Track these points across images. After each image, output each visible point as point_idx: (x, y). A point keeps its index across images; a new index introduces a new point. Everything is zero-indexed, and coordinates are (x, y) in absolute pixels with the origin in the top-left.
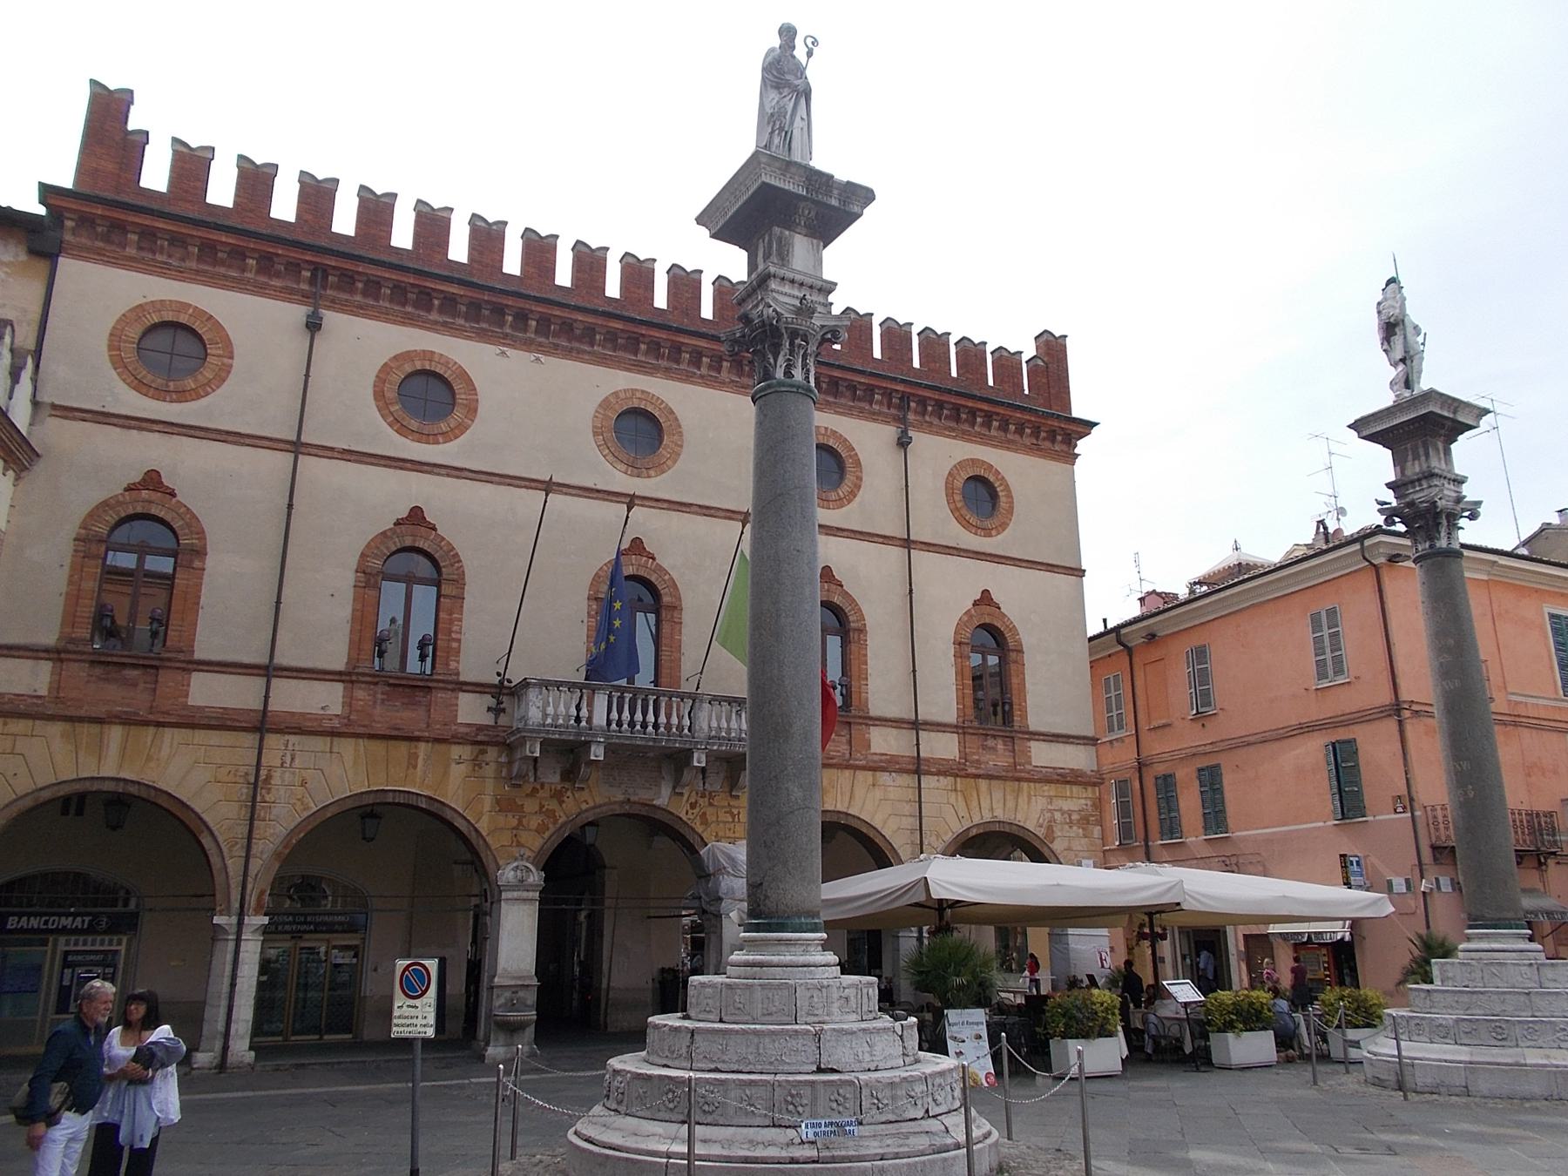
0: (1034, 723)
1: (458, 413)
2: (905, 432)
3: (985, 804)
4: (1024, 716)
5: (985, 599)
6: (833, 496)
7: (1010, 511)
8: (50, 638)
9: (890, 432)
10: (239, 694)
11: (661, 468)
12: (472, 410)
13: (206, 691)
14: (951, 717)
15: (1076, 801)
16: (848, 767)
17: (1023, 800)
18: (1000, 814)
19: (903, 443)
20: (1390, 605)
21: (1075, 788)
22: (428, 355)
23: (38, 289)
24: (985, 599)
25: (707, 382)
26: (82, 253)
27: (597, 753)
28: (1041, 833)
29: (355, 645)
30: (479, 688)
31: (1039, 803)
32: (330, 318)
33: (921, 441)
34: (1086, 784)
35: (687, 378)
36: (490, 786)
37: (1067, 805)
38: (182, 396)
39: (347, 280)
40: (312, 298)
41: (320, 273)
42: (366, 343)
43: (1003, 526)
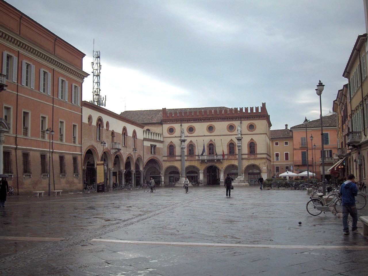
0: (258, 153)
1: (194, 131)
2: (241, 122)
3: (251, 162)
4: (257, 151)
5: (252, 139)
6: (232, 131)
7: (256, 128)
8: (166, 155)
9: (240, 122)
10: (179, 158)
11: (213, 132)
12: (195, 130)
13: (177, 158)
14: (247, 153)
15: (264, 161)
16: (234, 160)
17: (256, 161)
18: (253, 163)
19: (241, 123)
20: (307, 134)
21: (264, 160)
22: (191, 126)
23: (162, 127)
24: (252, 139)
25: (218, 121)
26: (164, 124)
27: (206, 161)
28: (258, 165)
29: (187, 153)
30: (197, 156)
31: (259, 161)
32: (183, 124)
33: (243, 122)
34: (264, 159)
35: (215, 122)
36: (199, 164)
37: (262, 161)
38: (172, 134)
39: (183, 121)
40: (181, 123)
41: (181, 121)
42: (186, 126)
43: (254, 130)
